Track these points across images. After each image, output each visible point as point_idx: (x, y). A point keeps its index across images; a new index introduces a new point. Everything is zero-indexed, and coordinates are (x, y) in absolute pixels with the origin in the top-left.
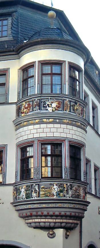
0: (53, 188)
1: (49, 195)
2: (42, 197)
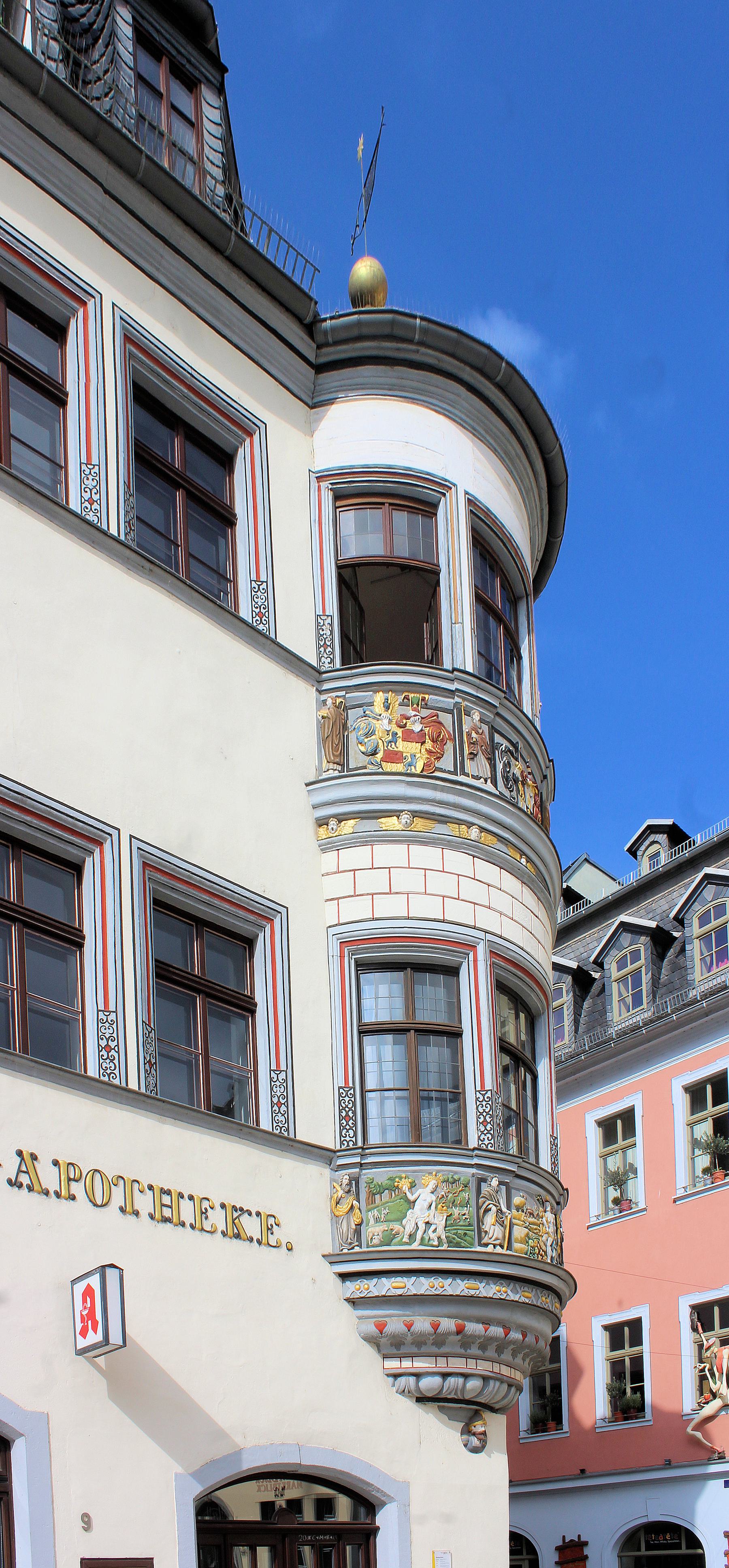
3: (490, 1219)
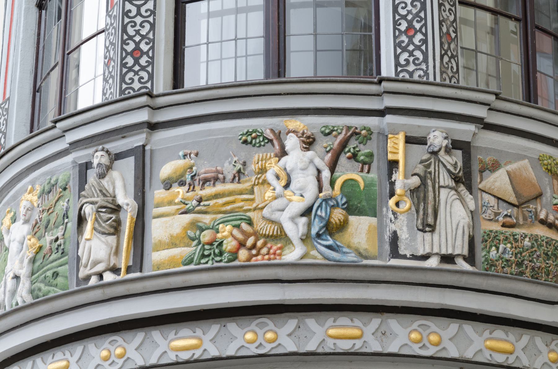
0: (270, 176)
1: (229, 245)
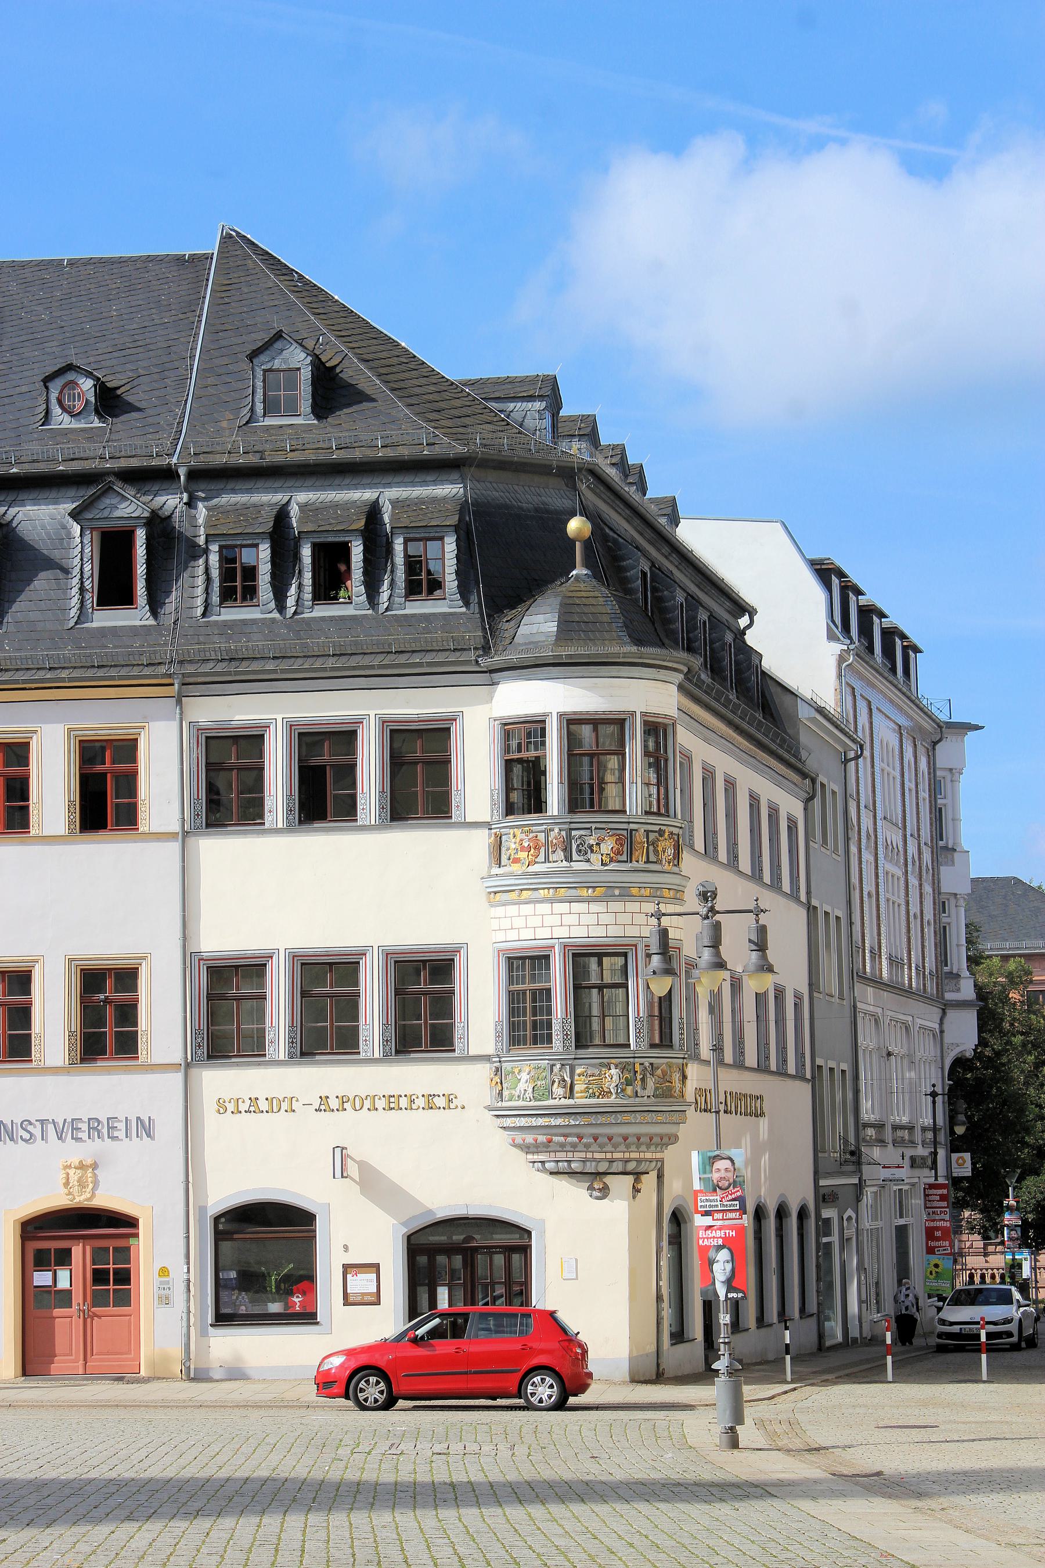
1: (597, 1094)
2: (582, 1097)
3: (556, 1085)
